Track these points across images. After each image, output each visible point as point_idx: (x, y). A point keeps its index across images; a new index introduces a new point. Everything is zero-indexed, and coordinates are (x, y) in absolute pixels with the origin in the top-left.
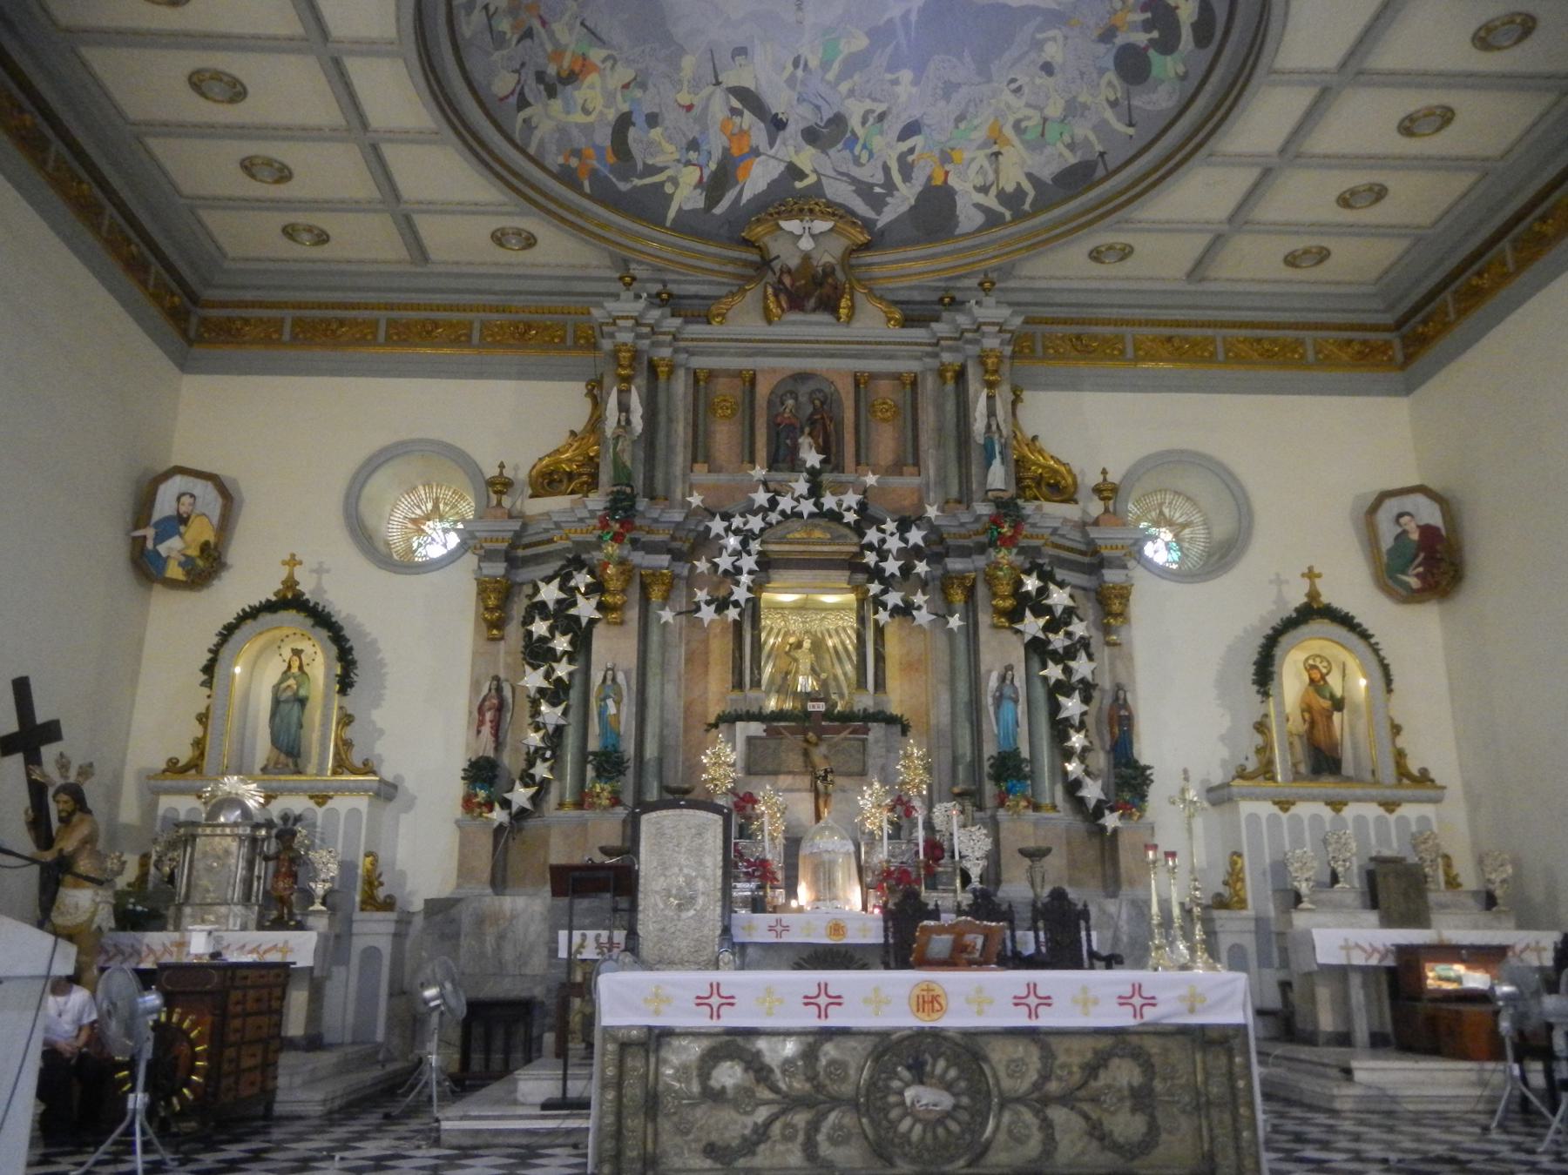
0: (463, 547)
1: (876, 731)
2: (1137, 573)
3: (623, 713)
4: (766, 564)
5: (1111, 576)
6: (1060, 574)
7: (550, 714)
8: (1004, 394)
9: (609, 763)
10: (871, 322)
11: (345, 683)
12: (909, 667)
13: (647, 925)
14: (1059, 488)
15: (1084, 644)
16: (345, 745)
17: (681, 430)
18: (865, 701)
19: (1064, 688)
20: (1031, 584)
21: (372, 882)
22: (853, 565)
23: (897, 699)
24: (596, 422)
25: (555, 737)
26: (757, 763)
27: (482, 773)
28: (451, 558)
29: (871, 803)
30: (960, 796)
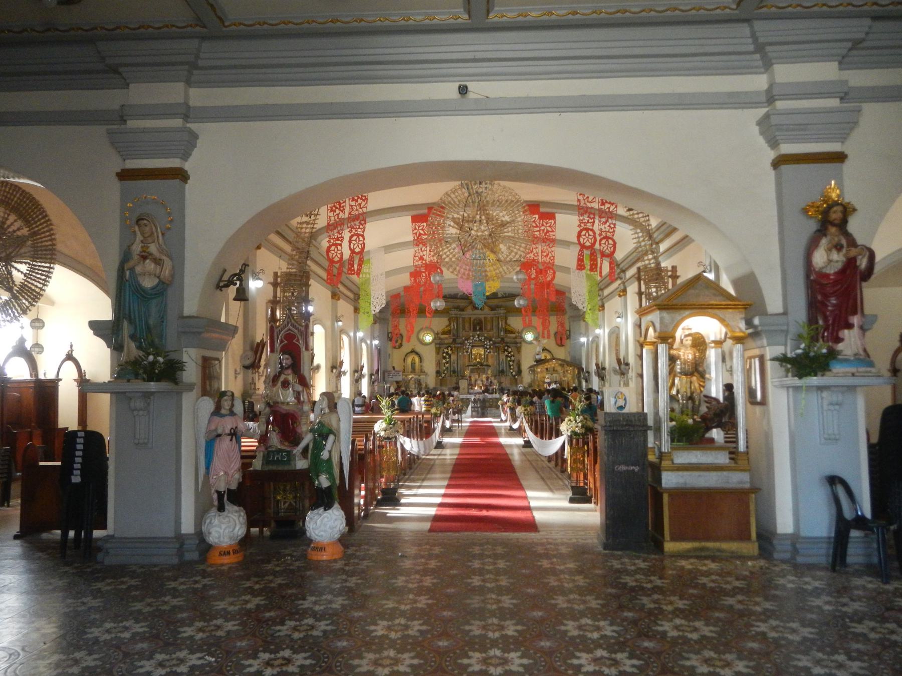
3: (455, 365)
4: (473, 346)
5: (519, 345)
8: (504, 321)
9: (454, 372)
11: (421, 362)
12: (492, 357)
14: (512, 332)
15: (513, 356)
16: (421, 370)
17: (461, 326)
18: (485, 363)
19: (510, 361)
21: (426, 386)
22: (483, 346)
23: (490, 362)
24: (450, 325)
25: (447, 368)
26: (472, 371)
27: (438, 372)
28: (431, 343)
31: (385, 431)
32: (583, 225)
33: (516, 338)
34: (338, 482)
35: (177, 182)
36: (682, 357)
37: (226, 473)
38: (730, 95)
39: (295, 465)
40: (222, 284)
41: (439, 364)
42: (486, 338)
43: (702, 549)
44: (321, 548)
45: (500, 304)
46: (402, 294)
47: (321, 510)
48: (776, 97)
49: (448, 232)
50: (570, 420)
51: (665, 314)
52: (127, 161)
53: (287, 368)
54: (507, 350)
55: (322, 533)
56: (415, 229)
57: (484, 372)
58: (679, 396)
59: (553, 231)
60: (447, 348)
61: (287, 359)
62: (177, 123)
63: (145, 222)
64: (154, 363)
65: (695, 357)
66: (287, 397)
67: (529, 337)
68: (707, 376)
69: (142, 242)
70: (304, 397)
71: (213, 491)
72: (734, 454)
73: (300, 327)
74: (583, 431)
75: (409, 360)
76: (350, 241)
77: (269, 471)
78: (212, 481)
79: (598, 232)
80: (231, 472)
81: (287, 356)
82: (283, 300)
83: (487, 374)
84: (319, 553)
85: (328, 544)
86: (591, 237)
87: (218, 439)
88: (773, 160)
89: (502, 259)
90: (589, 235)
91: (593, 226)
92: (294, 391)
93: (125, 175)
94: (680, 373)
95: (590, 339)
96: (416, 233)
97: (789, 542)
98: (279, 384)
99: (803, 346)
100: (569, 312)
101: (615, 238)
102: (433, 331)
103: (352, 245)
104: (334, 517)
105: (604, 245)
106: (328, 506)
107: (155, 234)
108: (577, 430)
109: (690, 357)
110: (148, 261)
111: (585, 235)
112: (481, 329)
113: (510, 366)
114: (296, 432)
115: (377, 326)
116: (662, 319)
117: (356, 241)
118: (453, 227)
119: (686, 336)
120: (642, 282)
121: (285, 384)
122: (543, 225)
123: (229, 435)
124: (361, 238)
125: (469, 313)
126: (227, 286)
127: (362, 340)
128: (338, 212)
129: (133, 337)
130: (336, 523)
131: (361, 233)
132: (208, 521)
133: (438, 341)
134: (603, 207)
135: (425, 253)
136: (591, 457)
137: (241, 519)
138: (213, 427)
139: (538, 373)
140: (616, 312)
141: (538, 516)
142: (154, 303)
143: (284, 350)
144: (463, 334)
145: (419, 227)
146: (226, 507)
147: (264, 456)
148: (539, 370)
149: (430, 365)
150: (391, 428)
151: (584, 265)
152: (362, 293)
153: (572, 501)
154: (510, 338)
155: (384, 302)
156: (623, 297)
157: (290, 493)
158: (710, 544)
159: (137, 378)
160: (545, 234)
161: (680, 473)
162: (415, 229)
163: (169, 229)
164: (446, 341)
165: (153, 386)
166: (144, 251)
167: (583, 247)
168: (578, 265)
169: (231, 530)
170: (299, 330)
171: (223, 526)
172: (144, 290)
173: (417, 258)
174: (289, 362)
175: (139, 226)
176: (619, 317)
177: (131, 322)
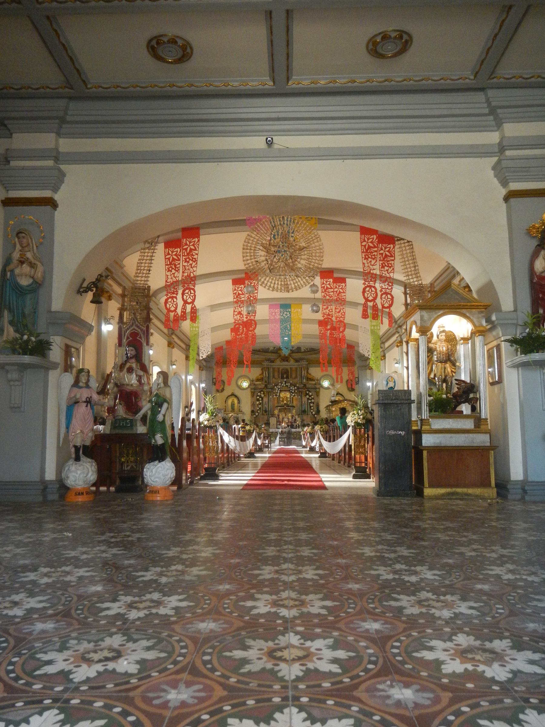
0: (249, 387)
1: (291, 408)
2: (321, 390)
3: (266, 406)
4: (281, 391)
5: (318, 390)
6: (311, 390)
7: (260, 406)
9: (266, 411)
10: (292, 362)
12: (296, 399)
13: (271, 426)
15: (313, 398)
16: (239, 409)
17: (272, 375)
18: (290, 405)
19: (311, 403)
20: (308, 392)
22: (289, 391)
23: (294, 404)
24: (263, 373)
25: (260, 408)
26: (280, 411)
27: (253, 412)
28: (247, 389)
29: (290, 415)
30: (299, 415)
31: (208, 421)
32: (367, 283)
33: (315, 384)
34: (170, 441)
35: (49, 208)
36: (438, 349)
37: (82, 432)
38: (472, 146)
39: (137, 430)
40: (81, 290)
41: (253, 405)
42: (291, 384)
43: (453, 494)
44: (155, 492)
45: (303, 357)
46: (225, 347)
47: (157, 462)
48: (505, 148)
49: (258, 254)
50: (354, 414)
51: (425, 314)
52: (9, 192)
53: (131, 358)
54: (308, 394)
55: (157, 479)
56: (235, 290)
57: (290, 411)
58: (436, 379)
59: (344, 292)
60: (260, 392)
61: (132, 350)
62: (50, 163)
63: (23, 235)
64: (29, 340)
65: (448, 349)
66: (132, 380)
67: (326, 384)
68: (458, 364)
69: (20, 251)
70: (144, 380)
71: (71, 446)
72: (479, 422)
73: (142, 328)
74: (364, 421)
75: (230, 402)
76: (183, 294)
77: (116, 434)
78: (71, 438)
79: (379, 289)
80: (86, 431)
81: (131, 348)
82: (130, 308)
83: (292, 413)
84: (155, 495)
85: (162, 488)
86: (373, 292)
87: (76, 405)
88: (505, 196)
89: (300, 275)
90: (372, 291)
91: (375, 284)
92: (137, 375)
93: (8, 202)
94: (437, 361)
95: (375, 384)
96: (235, 293)
97: (519, 486)
98: (125, 370)
99: (527, 330)
100: (358, 363)
101: (392, 293)
102: (249, 379)
103: (185, 297)
104: (167, 467)
105: (384, 299)
106: (161, 459)
107: (31, 245)
108: (359, 421)
109: (444, 349)
110: (24, 265)
111: (368, 291)
112: (287, 378)
113: (311, 407)
114: (138, 406)
115: (204, 372)
116: (422, 317)
117: (188, 293)
118: (262, 251)
119: (441, 332)
120: (408, 296)
121: (130, 370)
122: (336, 288)
123: (85, 402)
124: (192, 292)
125: (279, 364)
126: (86, 292)
127: (192, 383)
128: (173, 271)
129: (11, 323)
130: (168, 471)
131: (192, 287)
132: (67, 468)
133: (253, 387)
134: (383, 269)
135: (242, 309)
136: (370, 443)
137: (93, 468)
138: (72, 395)
139: (332, 411)
140: (395, 359)
141: (327, 484)
142: (29, 297)
143: (129, 345)
144: (272, 380)
145: (238, 288)
146: (82, 459)
147: (112, 422)
148: (334, 409)
149: (246, 407)
150: (213, 419)
151: (367, 315)
152: (192, 344)
153: (355, 477)
154: (310, 384)
155: (210, 350)
156: (400, 347)
157: (132, 456)
158: (459, 490)
159: (14, 354)
160: (338, 295)
161: (437, 435)
162: (235, 290)
163: (41, 244)
164: (260, 387)
165: (27, 359)
166: (22, 258)
167: (367, 300)
168: (363, 314)
169: (85, 475)
170: (141, 330)
171: (79, 472)
172: (21, 287)
173: (236, 313)
174: (134, 353)
175: (19, 238)
176: (397, 363)
177: (10, 310)
